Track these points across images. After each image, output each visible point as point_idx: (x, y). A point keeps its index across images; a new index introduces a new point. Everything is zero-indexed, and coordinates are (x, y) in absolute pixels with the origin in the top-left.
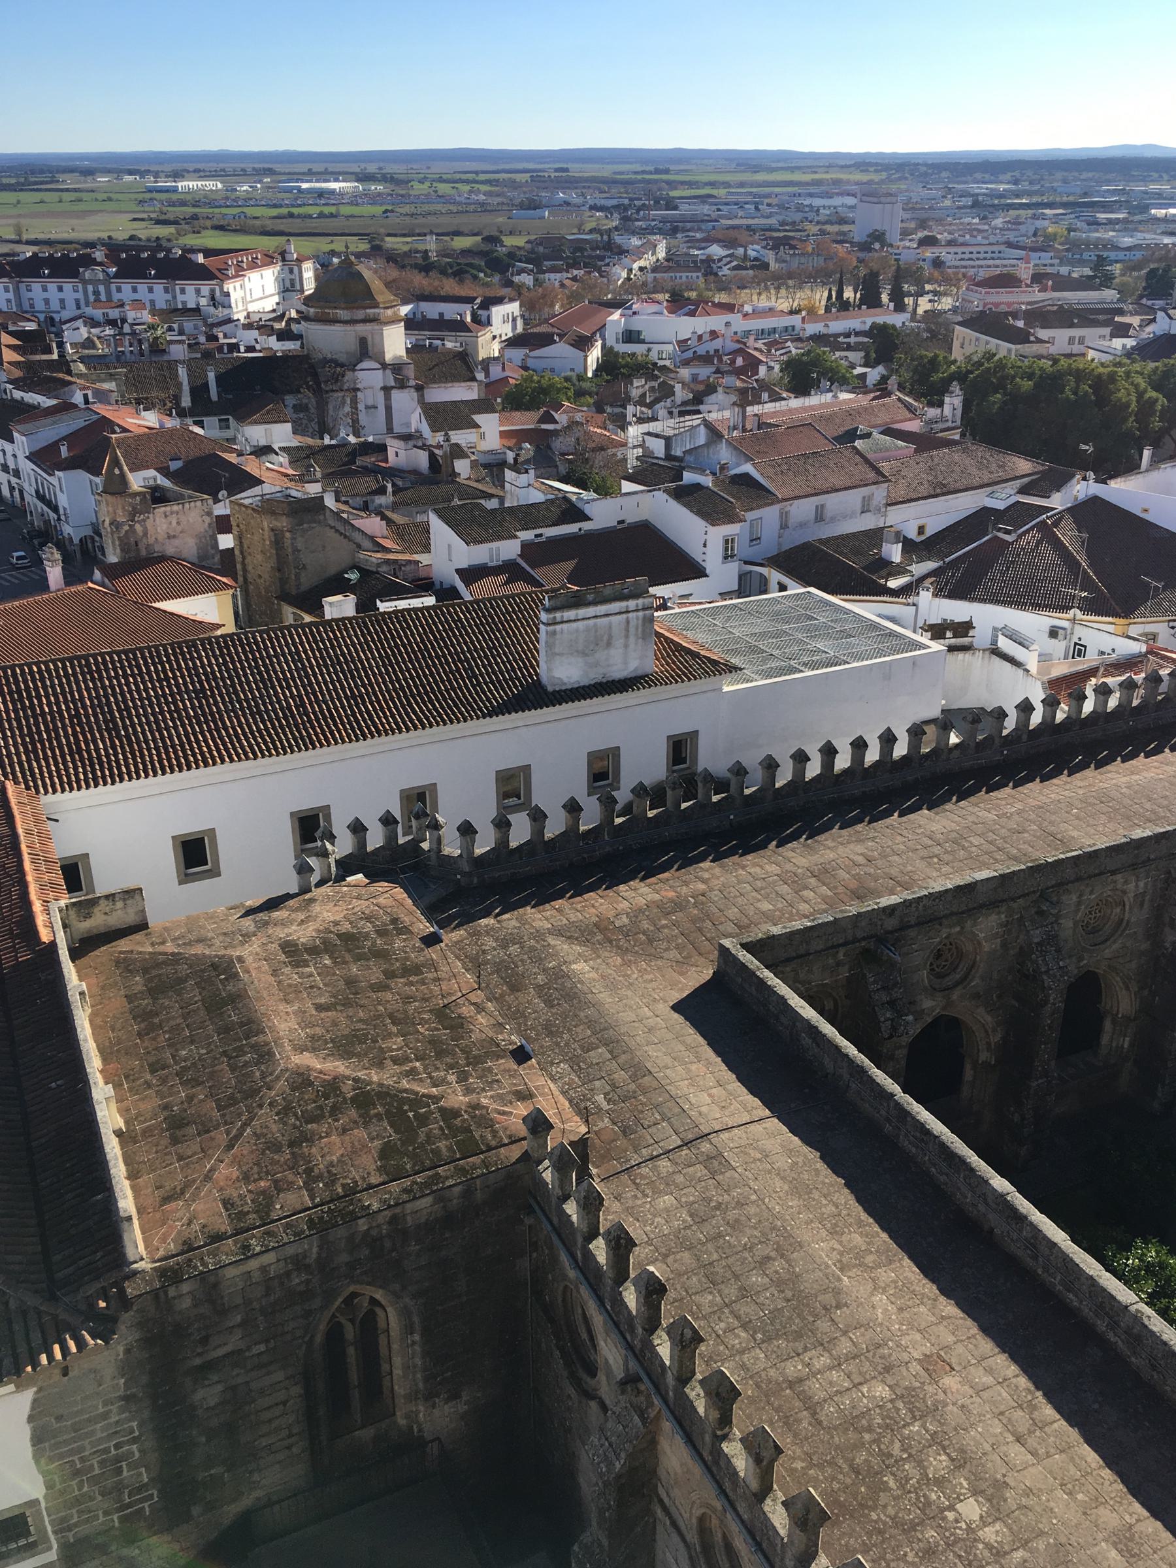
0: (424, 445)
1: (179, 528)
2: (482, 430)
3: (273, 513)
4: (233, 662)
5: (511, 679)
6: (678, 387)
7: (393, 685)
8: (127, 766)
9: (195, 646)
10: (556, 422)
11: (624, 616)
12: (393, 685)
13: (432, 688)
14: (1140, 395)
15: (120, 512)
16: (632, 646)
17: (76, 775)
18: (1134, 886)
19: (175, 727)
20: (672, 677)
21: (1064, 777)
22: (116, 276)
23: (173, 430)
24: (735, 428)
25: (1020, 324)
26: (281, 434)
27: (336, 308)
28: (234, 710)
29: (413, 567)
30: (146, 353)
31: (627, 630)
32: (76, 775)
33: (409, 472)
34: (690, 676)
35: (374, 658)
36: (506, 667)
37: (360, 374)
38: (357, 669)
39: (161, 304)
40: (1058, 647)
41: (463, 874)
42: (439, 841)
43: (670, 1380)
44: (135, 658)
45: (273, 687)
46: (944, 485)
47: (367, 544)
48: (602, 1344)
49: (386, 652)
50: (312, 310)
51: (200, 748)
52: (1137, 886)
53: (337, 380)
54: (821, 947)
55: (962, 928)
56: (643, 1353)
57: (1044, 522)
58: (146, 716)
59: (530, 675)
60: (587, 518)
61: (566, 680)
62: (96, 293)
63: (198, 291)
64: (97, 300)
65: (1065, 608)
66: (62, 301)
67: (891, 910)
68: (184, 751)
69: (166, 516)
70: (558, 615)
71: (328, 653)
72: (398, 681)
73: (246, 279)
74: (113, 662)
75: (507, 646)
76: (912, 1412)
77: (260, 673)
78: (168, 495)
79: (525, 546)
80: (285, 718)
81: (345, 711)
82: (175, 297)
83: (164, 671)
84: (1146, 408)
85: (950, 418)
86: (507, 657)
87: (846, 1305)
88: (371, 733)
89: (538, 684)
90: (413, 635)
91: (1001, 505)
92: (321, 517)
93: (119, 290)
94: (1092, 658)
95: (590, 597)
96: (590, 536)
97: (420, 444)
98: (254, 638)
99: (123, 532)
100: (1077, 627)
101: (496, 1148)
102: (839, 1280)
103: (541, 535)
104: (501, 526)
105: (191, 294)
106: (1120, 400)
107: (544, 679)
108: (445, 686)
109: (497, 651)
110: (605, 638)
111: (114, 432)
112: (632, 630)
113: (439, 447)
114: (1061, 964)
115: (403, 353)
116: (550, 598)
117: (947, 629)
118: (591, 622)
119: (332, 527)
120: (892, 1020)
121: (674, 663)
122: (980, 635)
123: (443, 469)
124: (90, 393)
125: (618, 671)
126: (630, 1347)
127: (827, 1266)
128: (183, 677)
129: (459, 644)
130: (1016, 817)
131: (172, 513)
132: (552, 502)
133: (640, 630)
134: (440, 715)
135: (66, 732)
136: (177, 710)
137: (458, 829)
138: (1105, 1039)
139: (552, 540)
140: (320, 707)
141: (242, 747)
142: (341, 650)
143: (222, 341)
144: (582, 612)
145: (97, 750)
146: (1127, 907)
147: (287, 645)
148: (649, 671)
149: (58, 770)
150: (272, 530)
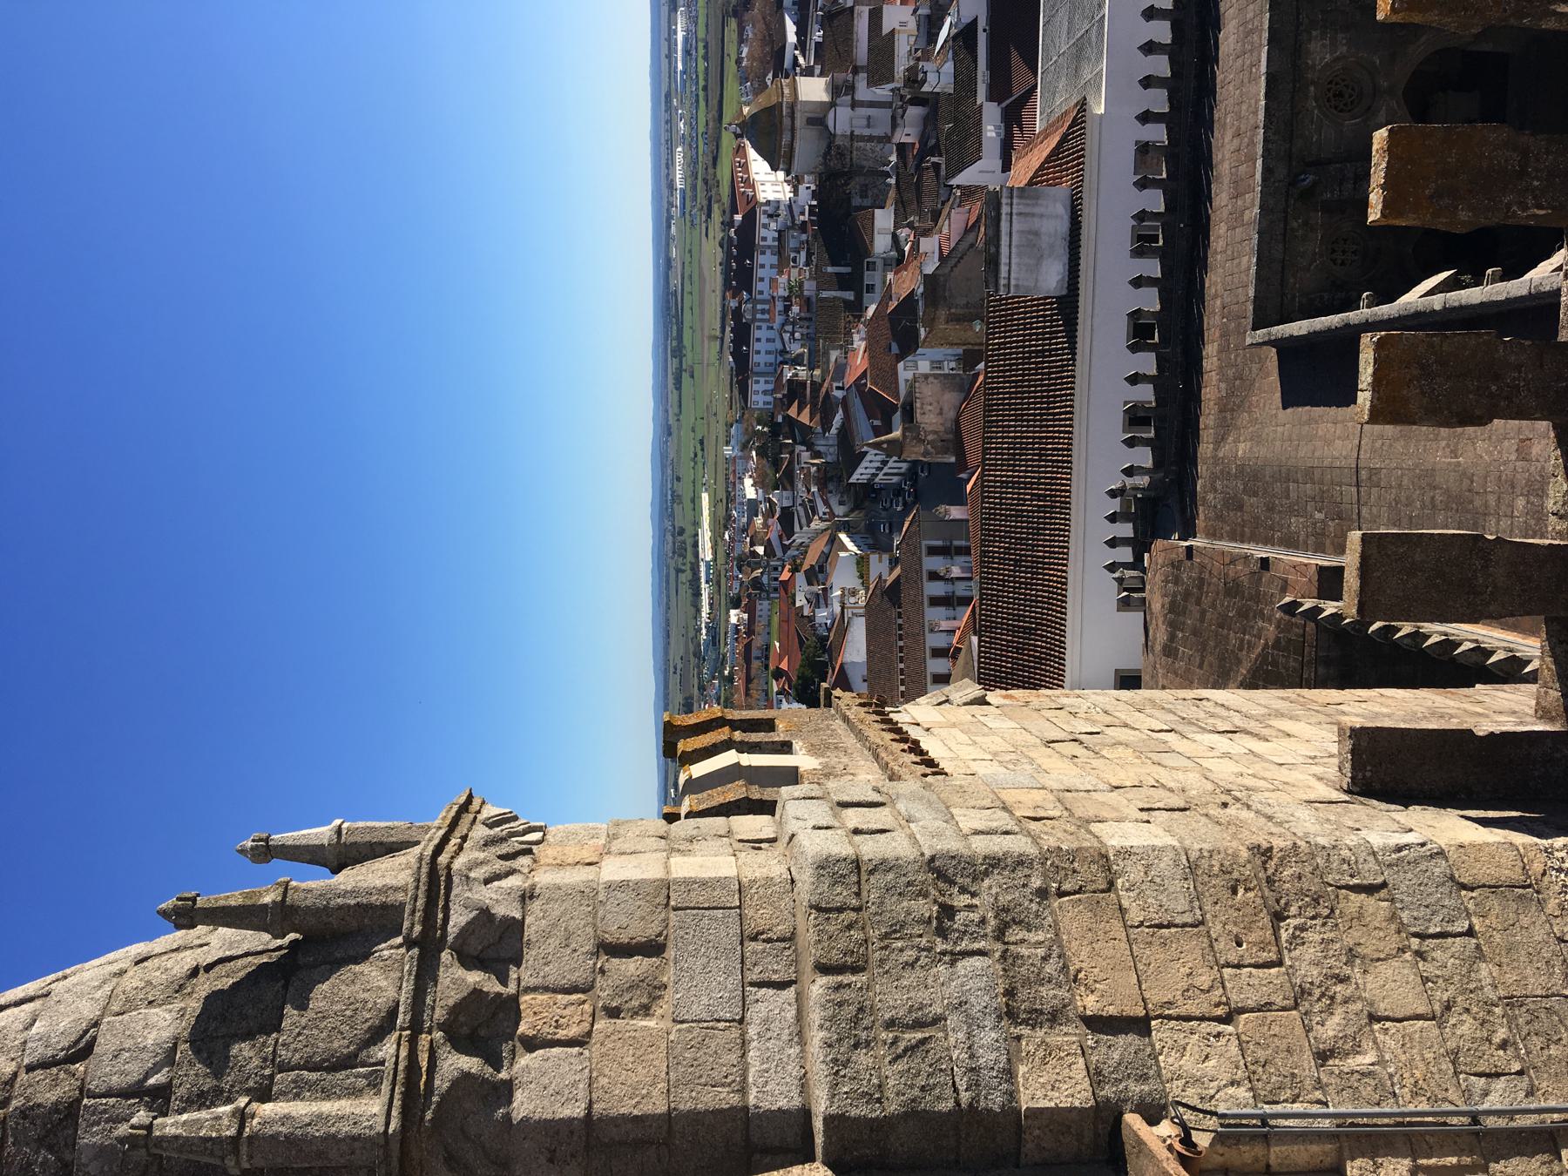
1: (935, 404)
2: (898, 28)
3: (933, 319)
4: (1001, 531)
7: (1038, 420)
8: (1056, 634)
9: (985, 552)
11: (1014, 217)
13: (1045, 391)
15: (916, 449)
17: (1055, 668)
19: (1037, 590)
20: (1078, 171)
22: (750, 292)
23: (867, 332)
26: (884, 219)
27: (781, 146)
28: (1033, 546)
30: (808, 315)
32: (1055, 668)
35: (1015, 426)
37: (839, 132)
38: (1021, 443)
39: (774, 260)
44: (987, 595)
45: (1023, 511)
47: (970, 238)
49: (1012, 415)
50: (781, 166)
51: (1054, 582)
53: (842, 155)
54: (1281, 246)
55: (1313, 83)
58: (1026, 606)
60: (975, 21)
61: (1060, 277)
62: (763, 312)
63: (766, 226)
64: (768, 312)
66: (768, 340)
67: (1267, 171)
68: (1054, 593)
69: (924, 413)
70: (1002, 282)
71: (1005, 460)
73: (757, 178)
74: (987, 610)
75: (1026, 313)
77: (1011, 516)
78: (909, 399)
79: (990, 98)
80: (1046, 512)
81: (1049, 466)
82: (769, 247)
83: (999, 580)
86: (1034, 317)
87: (1473, 475)
92: (942, 279)
93: (761, 293)
96: (992, 19)
97: (900, 111)
98: (986, 508)
99: (932, 450)
101: (1304, 631)
105: (767, 232)
108: (1045, 380)
109: (1028, 323)
110: (1031, 237)
111: (866, 384)
112: (1027, 210)
119: (952, 270)
121: (1067, 163)
124: (835, 385)
125: (1063, 226)
127: (1449, 463)
128: (1005, 570)
131: (922, 408)
132: (955, 55)
133: (1028, 202)
135: (1026, 660)
136: (1026, 584)
140: (1042, 483)
141: (1059, 553)
142: (1005, 449)
143: (806, 218)
144: (1004, 259)
145: (1042, 647)
147: (996, 487)
149: (1050, 678)
150: (947, 322)
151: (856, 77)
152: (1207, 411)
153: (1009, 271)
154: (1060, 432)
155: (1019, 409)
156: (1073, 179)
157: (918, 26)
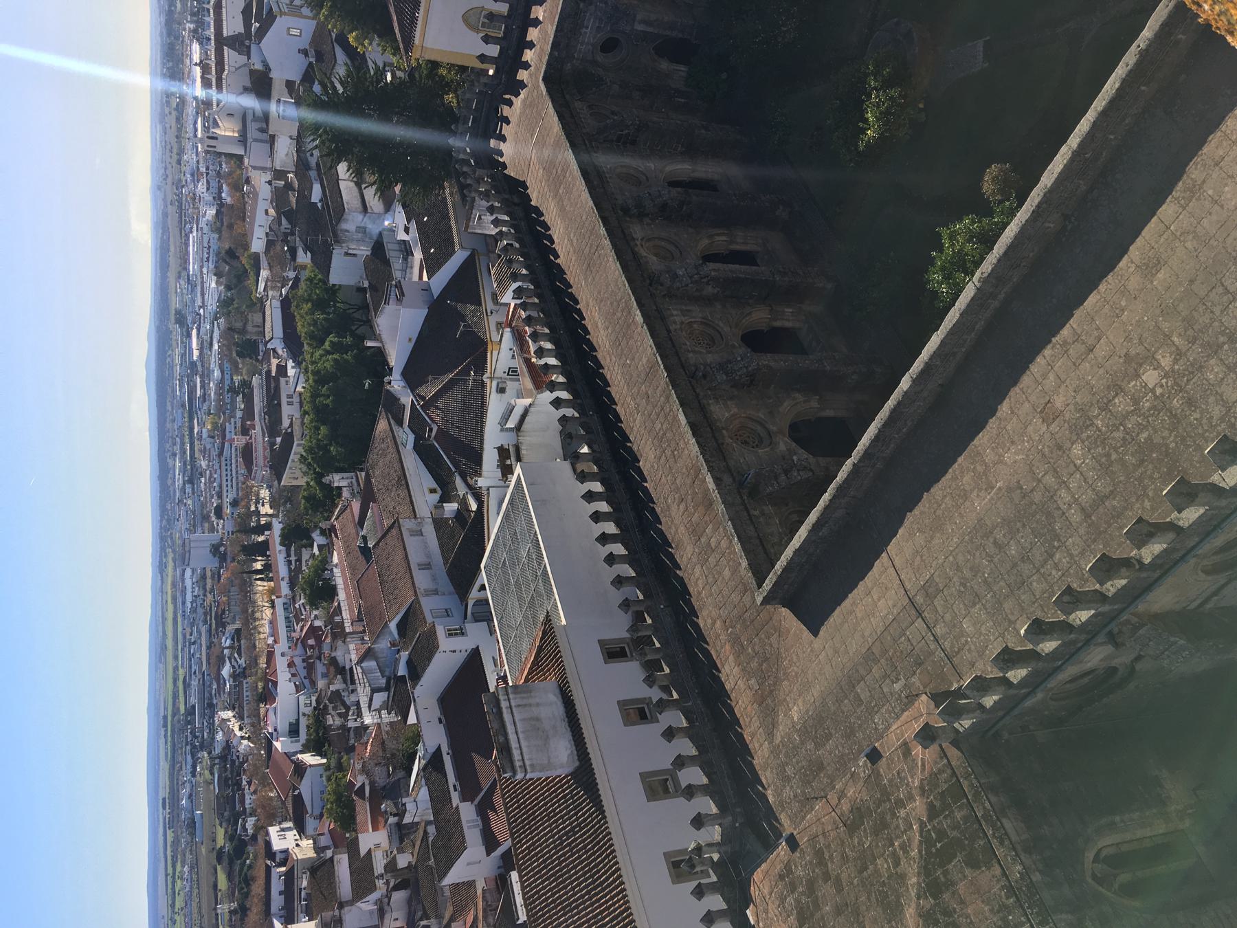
0: (387, 896)
2: (372, 847)
5: (572, 798)
6: (333, 688)
7: (587, 900)
10: (363, 785)
11: (514, 709)
12: (587, 900)
14: (328, 353)
16: (537, 700)
18: (677, 317)
21: (605, 371)
24: (363, 639)
25: (279, 440)
29: (487, 895)
31: (525, 705)
33: (410, 908)
34: (557, 652)
36: (563, 803)
40: (511, 386)
41: (735, 821)
42: (710, 845)
43: (1106, 608)
46: (399, 478)
48: (1089, 665)
49: (560, 911)
52: (676, 315)
54: (752, 528)
55: (723, 428)
56: (1090, 632)
57: (422, 407)
59: (568, 782)
60: (439, 749)
61: (569, 752)
65: (483, 385)
67: (717, 481)
70: (518, 764)
72: (582, 896)
76: (1087, 427)
79: (464, 799)
84: (336, 348)
85: (349, 481)
86: (555, 803)
87: (1018, 482)
88: (628, 916)
89: (574, 774)
90: (544, 888)
91: (412, 437)
94: (518, 363)
95: (501, 739)
97: (386, 900)
100: (496, 376)
101: (952, 769)
102: (1000, 489)
103: (454, 786)
104: (449, 821)
106: (332, 366)
107: (570, 770)
112: (525, 702)
113: (388, 883)
114: (739, 359)
115: (313, 923)
116: (505, 772)
117: (504, 464)
118: (521, 736)
120: (798, 470)
121: (547, 665)
122: (507, 440)
123: (405, 877)
125: (558, 709)
126: (1087, 643)
127: (992, 498)
129: (548, 846)
130: (637, 401)
134: (608, 856)
137: (698, 829)
138: (788, 324)
139: (458, 777)
146: (692, 320)
148: (555, 685)
151: (342, 911)
152: (747, 720)
153: (522, 754)
154: (612, 898)
155: (564, 901)
156: (555, 674)
157: (390, 842)
